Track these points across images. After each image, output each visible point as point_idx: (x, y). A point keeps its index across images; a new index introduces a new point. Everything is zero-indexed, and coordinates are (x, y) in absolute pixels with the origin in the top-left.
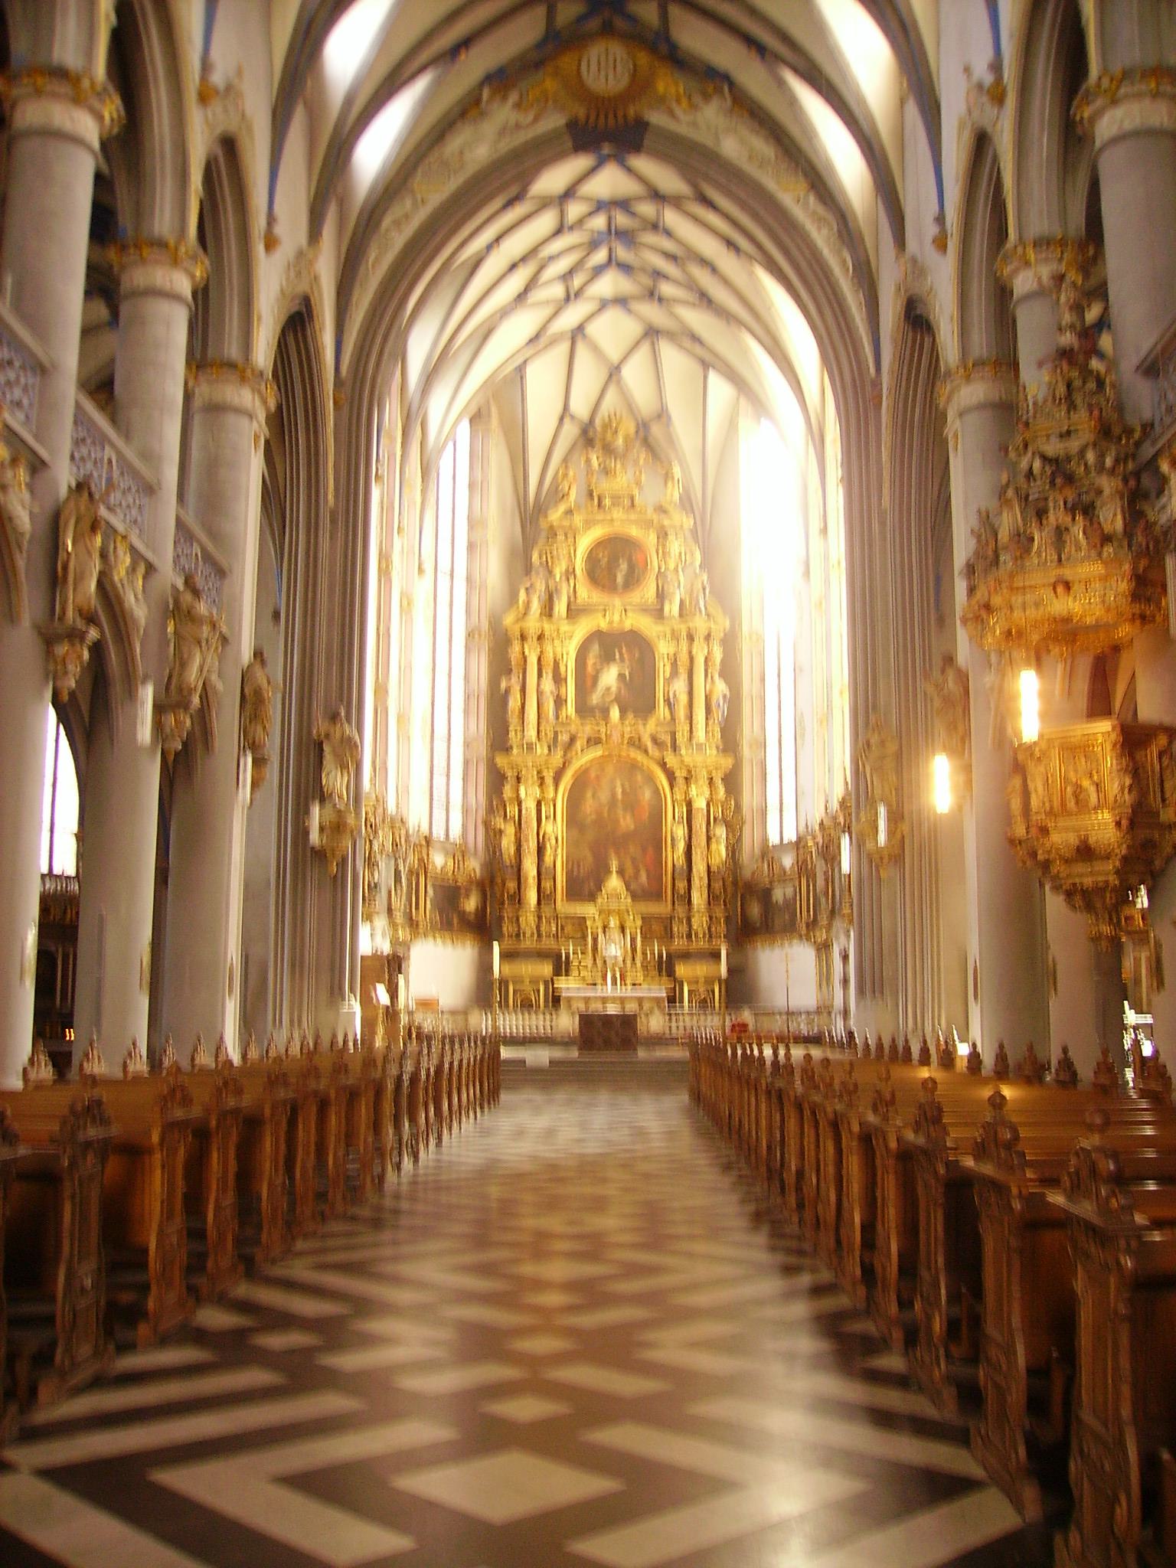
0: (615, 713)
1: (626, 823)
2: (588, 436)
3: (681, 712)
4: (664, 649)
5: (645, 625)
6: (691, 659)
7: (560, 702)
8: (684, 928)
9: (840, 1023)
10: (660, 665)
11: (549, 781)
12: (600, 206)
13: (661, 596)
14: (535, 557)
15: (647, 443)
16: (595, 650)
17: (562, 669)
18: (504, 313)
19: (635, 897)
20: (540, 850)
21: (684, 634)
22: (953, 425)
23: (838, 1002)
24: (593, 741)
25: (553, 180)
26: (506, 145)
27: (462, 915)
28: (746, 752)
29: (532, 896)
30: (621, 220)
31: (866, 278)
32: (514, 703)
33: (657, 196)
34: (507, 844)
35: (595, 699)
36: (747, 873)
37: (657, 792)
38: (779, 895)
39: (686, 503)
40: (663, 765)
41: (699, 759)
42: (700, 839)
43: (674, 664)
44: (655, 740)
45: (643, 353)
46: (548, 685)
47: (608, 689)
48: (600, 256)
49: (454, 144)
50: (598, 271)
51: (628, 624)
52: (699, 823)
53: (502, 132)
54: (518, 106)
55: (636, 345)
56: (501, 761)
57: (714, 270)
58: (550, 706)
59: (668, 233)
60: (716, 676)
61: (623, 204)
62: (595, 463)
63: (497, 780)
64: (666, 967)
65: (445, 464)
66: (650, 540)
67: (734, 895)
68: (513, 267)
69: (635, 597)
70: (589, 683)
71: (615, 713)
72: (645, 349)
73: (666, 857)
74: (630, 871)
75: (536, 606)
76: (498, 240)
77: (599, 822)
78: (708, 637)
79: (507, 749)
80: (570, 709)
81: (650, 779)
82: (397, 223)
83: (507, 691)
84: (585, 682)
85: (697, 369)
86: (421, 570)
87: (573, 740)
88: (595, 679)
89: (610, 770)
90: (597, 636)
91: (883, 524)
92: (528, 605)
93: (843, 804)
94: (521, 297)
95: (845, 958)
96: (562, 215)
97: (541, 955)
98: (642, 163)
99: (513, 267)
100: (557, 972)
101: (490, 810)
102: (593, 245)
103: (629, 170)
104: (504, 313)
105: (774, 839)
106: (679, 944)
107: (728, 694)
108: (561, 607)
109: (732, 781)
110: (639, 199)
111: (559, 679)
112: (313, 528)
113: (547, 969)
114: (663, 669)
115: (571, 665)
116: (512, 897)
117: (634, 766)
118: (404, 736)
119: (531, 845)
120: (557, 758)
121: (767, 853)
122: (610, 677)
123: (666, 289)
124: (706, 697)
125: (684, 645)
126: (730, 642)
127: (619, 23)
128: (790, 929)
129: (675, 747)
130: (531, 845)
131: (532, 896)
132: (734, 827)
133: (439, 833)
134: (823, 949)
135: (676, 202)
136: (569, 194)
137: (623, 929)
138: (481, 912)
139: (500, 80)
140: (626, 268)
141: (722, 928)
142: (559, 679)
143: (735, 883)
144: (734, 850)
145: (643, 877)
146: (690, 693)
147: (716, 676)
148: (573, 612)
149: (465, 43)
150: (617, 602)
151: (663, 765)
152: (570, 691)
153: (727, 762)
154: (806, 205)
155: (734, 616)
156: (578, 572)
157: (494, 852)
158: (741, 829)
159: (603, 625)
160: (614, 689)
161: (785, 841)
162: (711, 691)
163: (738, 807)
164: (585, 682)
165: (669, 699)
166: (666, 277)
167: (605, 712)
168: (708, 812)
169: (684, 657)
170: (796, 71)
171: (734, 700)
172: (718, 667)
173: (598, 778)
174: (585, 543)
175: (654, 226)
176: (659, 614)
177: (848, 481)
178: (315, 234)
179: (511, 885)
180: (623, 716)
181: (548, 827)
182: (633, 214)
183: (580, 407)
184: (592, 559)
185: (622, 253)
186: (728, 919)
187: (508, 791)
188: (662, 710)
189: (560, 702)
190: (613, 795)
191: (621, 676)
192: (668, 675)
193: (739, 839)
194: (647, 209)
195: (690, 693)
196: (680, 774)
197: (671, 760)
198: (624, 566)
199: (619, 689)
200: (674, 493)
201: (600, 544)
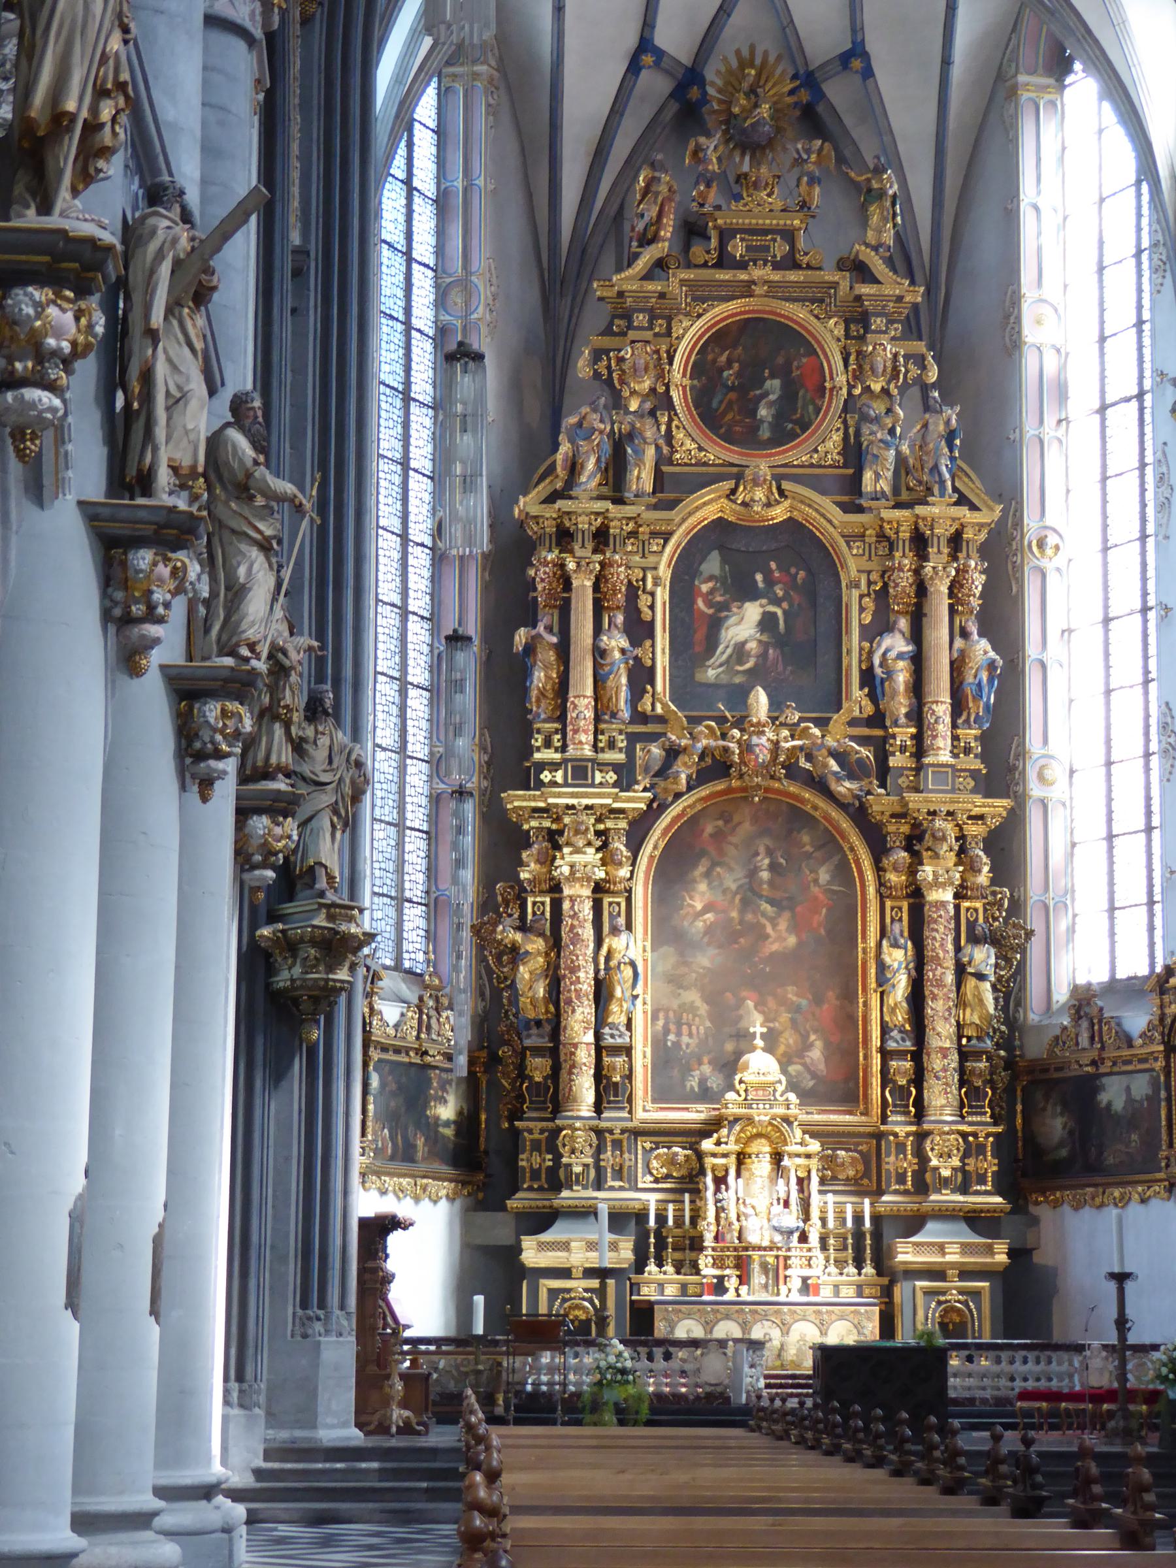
6: (922, 589)
7: (642, 676)
8: (908, 1163)
10: (852, 597)
16: (713, 564)
17: (644, 601)
20: (602, 993)
21: (905, 535)
27: (431, 1127)
32: (541, 678)
36: (1035, 1048)
37: (844, 872)
40: (859, 813)
43: (882, 596)
44: (840, 756)
47: (740, 648)
51: (779, 513)
60: (973, 629)
62: (714, 166)
67: (1010, 1090)
69: (797, 455)
70: (700, 635)
73: (865, 1004)
74: (789, 1039)
75: (590, 475)
78: (956, 541)
79: (527, 778)
81: (831, 843)
83: (530, 649)
87: (673, 753)
88: (715, 625)
89: (747, 827)
92: (574, 468)
101: (488, 906)
107: (1000, 663)
111: (639, 630)
115: (662, 595)
116: (536, 1088)
120: (636, 800)
124: (952, 663)
125: (905, 560)
129: (883, 772)
141: (989, 1165)
142: (639, 630)
143: (1009, 1064)
145: (816, 1054)
147: (973, 629)
151: (859, 813)
156: (675, 395)
157: (496, 994)
158: (1024, 952)
160: (752, 646)
161: (1121, 975)
162: (962, 653)
165: (871, 668)
168: (957, 908)
172: (975, 603)
173: (718, 836)
179: (538, 1068)
180: (776, 705)
184: (701, 368)
186: (1002, 1145)
188: (857, 700)
189: (642, 676)
190: (753, 873)
191: (767, 623)
192: (867, 618)
193: (1021, 970)
195: (918, 661)
196: (898, 830)
197: (881, 803)
198: (774, 385)
199: (763, 655)
201: (719, 338)
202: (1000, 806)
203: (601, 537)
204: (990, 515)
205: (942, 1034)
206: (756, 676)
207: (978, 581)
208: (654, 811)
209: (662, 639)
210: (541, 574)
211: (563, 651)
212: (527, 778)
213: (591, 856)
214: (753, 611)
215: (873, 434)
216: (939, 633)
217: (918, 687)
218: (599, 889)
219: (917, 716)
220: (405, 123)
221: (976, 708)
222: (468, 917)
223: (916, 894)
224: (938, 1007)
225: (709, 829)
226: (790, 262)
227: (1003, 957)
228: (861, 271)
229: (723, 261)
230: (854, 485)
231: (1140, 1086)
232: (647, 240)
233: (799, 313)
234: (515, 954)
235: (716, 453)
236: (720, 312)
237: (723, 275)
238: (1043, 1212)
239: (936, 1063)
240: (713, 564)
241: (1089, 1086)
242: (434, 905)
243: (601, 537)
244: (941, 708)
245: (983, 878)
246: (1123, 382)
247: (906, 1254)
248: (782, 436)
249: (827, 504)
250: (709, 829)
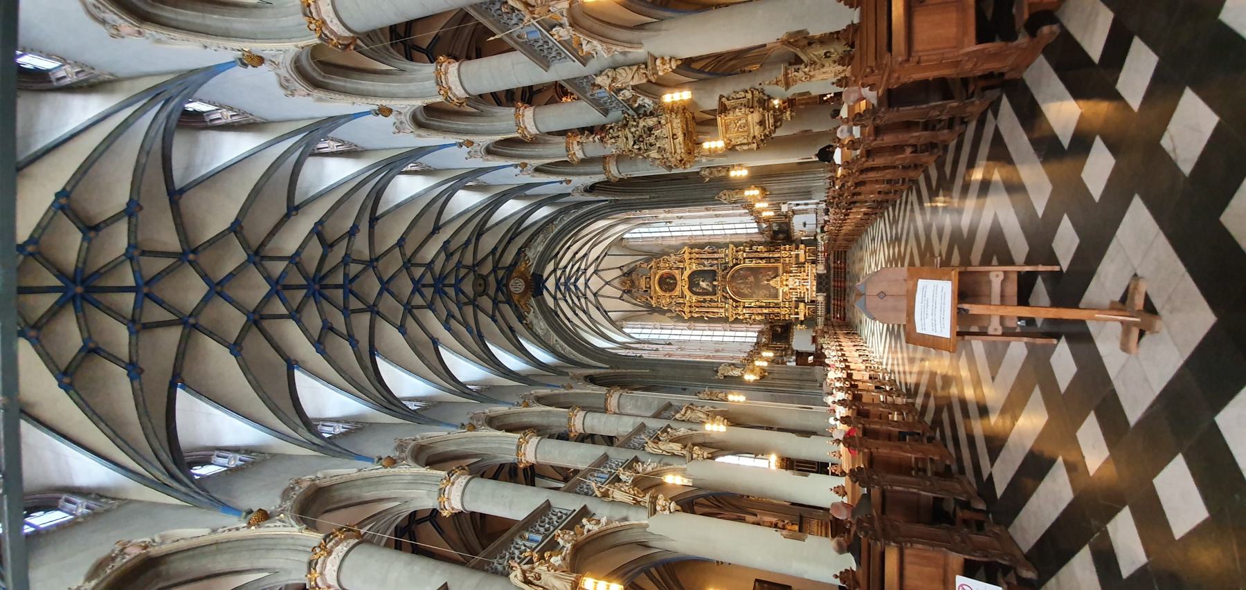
0: (715, 283)
1: (751, 279)
2: (629, 292)
3: (716, 262)
4: (694, 267)
5: (687, 273)
8: (787, 259)
9: (820, 205)
11: (737, 304)
12: (557, 287)
13: (678, 268)
14: (666, 308)
15: (629, 274)
18: (590, 317)
19: (777, 276)
22: (623, 176)
23: (814, 206)
24: (724, 290)
25: (550, 302)
26: (540, 316)
28: (728, 240)
29: (777, 310)
30: (562, 280)
31: (579, 205)
33: (555, 271)
34: (759, 318)
35: (711, 289)
37: (741, 269)
38: (776, 228)
39: (648, 261)
40: (732, 267)
41: (730, 256)
42: (756, 255)
44: (723, 271)
45: (601, 273)
46: (706, 305)
48: (573, 288)
49: (540, 332)
50: (576, 288)
51: (687, 279)
52: (751, 256)
53: (536, 317)
54: (528, 313)
55: (600, 277)
56: (731, 319)
57: (576, 253)
58: (713, 304)
59: (566, 267)
61: (558, 281)
63: (736, 321)
64: (800, 265)
65: (636, 336)
66: (660, 272)
68: (577, 315)
69: (678, 277)
71: (715, 283)
72: (600, 273)
76: (568, 319)
77: (750, 288)
79: (727, 318)
80: (713, 297)
81: (737, 271)
82: (564, 350)
84: (706, 293)
85: (607, 257)
86: (670, 344)
88: (704, 289)
90: (690, 289)
91: (654, 198)
93: (745, 208)
94: (584, 311)
95: (797, 205)
96: (560, 299)
97: (797, 307)
98: (545, 276)
99: (577, 315)
100: (804, 301)
101: (747, 323)
102: (569, 290)
103: (547, 279)
104: (590, 317)
105: (757, 230)
106: (793, 260)
108: (681, 301)
109: (737, 245)
110: (556, 276)
111: (705, 301)
112: (656, 377)
113: (802, 305)
114: (703, 268)
117: (732, 276)
118: (723, 350)
119: (759, 311)
121: (761, 232)
122: (703, 284)
123: (583, 267)
125: (693, 261)
126: (692, 247)
127: (504, 282)
128: (788, 224)
130: (759, 311)
131: (777, 310)
132: (751, 244)
133: (755, 340)
134: (794, 212)
135: (557, 265)
136: (555, 298)
137: (787, 280)
138: (781, 327)
139: (521, 318)
140: (577, 280)
144: (760, 244)
146: (708, 259)
148: (683, 296)
149: (511, 328)
150: (679, 283)
152: (708, 298)
153: (731, 246)
154: (557, 225)
155: (684, 245)
159: (686, 287)
163: (746, 242)
164: (706, 293)
166: (579, 268)
167: (715, 286)
169: (696, 261)
170: (518, 228)
171: (711, 244)
174: (660, 293)
175: (564, 271)
176: (683, 269)
177: (641, 209)
178: (567, 374)
180: (715, 280)
181: (753, 305)
182: (560, 278)
183: (619, 293)
185: (573, 280)
187: (741, 317)
188: (714, 268)
189: (711, 301)
191: (703, 281)
194: (559, 273)
197: (731, 264)
198: (668, 280)
200: (645, 265)
201: (661, 288)
202: (731, 246)
203: (690, 307)
204: (686, 248)
205: (766, 255)
206: (711, 283)
207: (696, 250)
208: (732, 298)
209: (706, 297)
210: (696, 315)
211: (707, 312)
212: (728, 318)
213: (740, 309)
214: (701, 283)
215: (675, 266)
216: (704, 256)
217: (712, 259)
218: (744, 307)
219: (717, 259)
220: (629, 335)
221: (716, 250)
222: (749, 326)
223: (744, 258)
224: (761, 255)
225: (734, 289)
226: (650, 278)
227: (754, 245)
228: (651, 268)
229: (650, 288)
230: (682, 268)
231: (774, 225)
232: (647, 299)
233: (657, 277)
234: (754, 320)
235: (678, 288)
236: (657, 288)
237: (652, 288)
238: (795, 238)
239: (771, 256)
240: (694, 289)
241: (774, 231)
242: (747, 331)
243: (690, 307)
244: (716, 256)
245: (742, 248)
246: (667, 229)
247: (802, 259)
248: (675, 279)
249: (685, 273)
250: (734, 289)
